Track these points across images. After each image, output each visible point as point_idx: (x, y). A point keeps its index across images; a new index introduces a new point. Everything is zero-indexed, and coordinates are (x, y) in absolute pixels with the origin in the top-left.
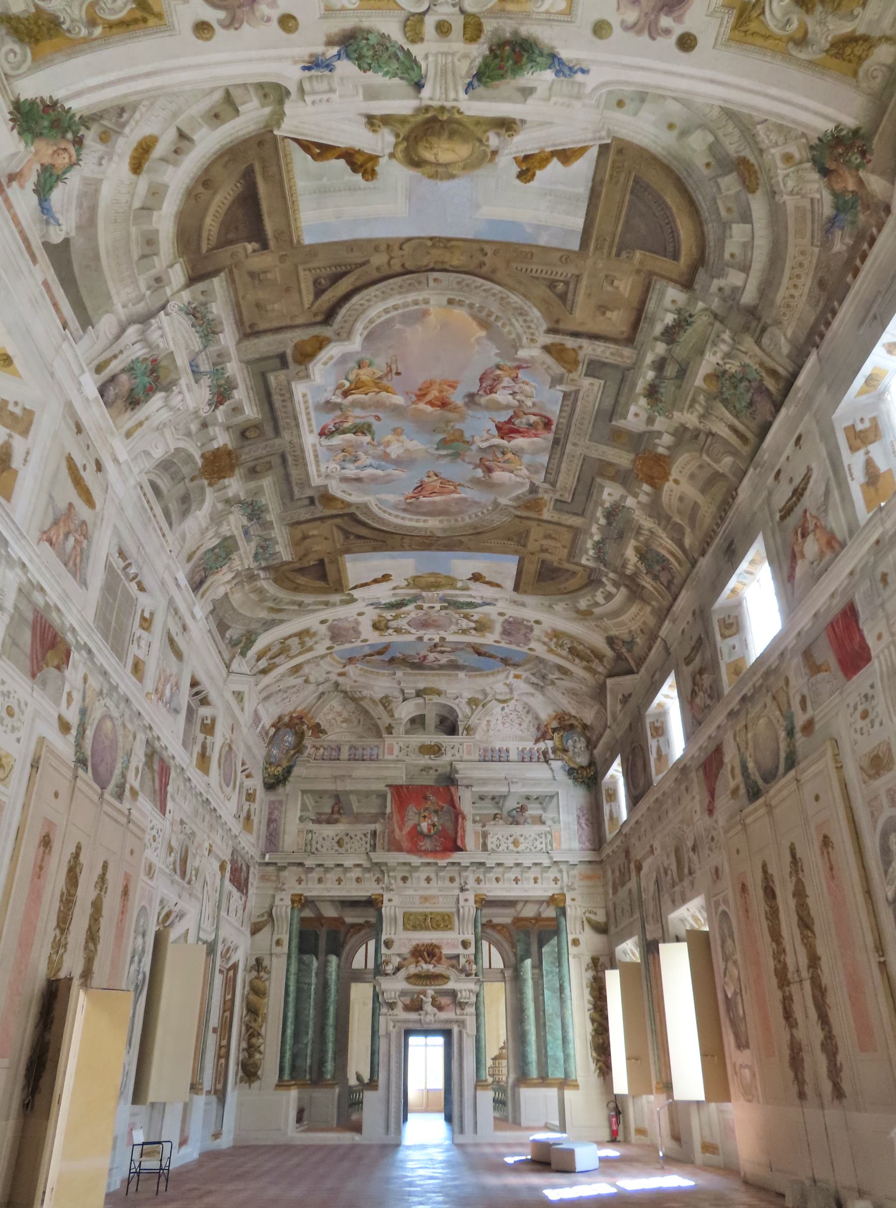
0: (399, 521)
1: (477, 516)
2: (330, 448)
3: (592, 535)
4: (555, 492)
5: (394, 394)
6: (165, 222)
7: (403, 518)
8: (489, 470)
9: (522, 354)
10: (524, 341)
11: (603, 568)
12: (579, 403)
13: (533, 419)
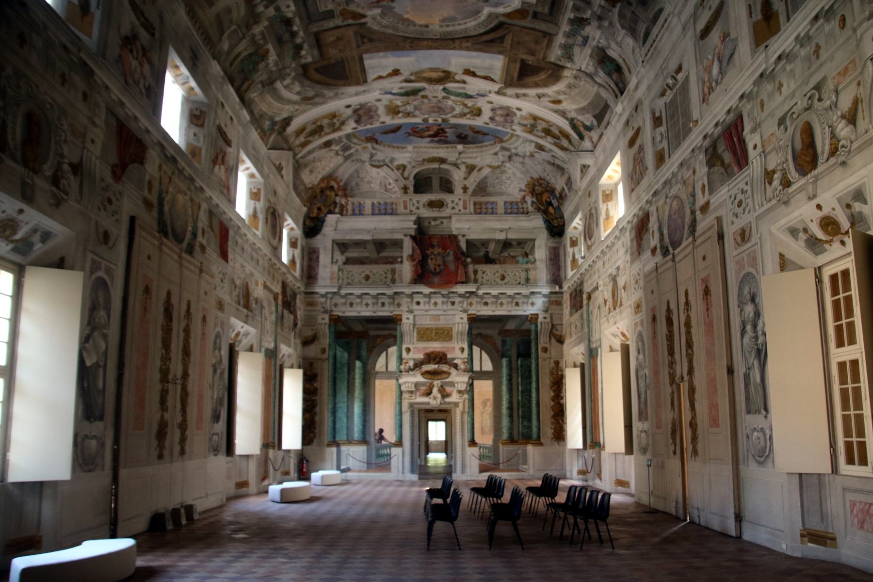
6: (560, 86)
9: (378, 11)
10: (379, 18)
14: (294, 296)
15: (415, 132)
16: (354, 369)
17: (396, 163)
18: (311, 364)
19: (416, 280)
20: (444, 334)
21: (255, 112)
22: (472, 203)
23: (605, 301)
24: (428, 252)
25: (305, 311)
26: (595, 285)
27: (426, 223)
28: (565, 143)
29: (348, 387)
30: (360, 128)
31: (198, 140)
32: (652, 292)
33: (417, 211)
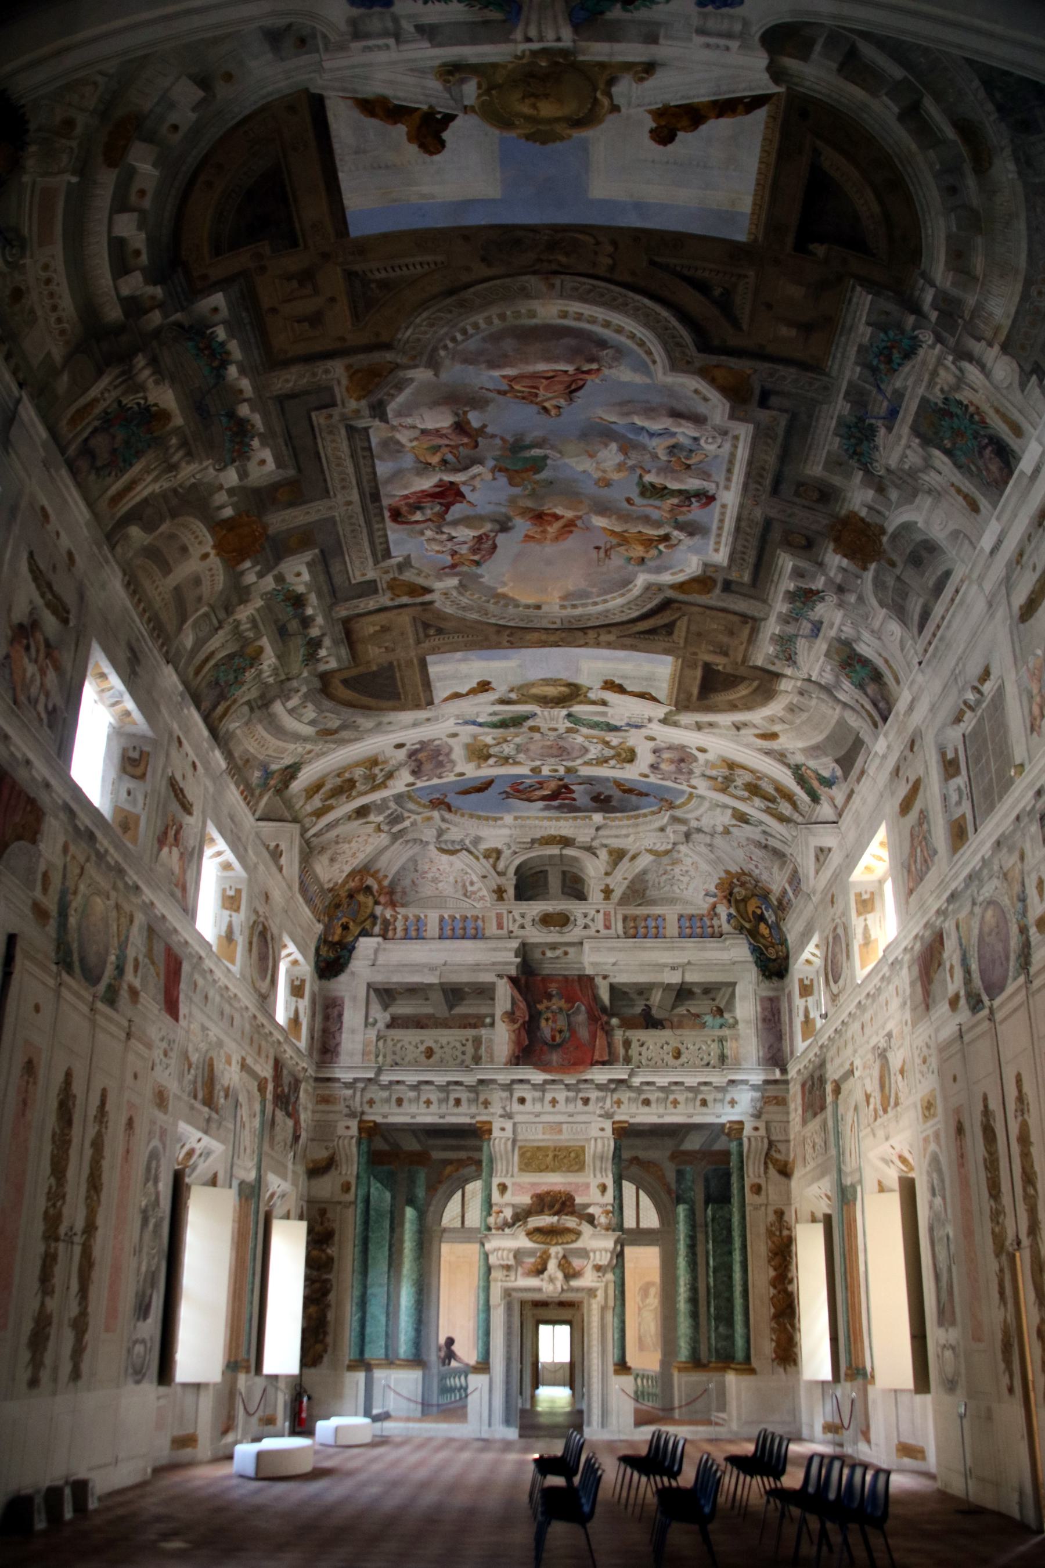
0: (617, 319)
1: (464, 332)
2: (706, 476)
3: (242, 371)
4: (344, 418)
5: (605, 529)
6: (775, 708)
7: (607, 324)
8: (461, 427)
10: (455, 593)
11: (178, 316)
12: (368, 551)
13: (418, 516)
14: (296, 1083)
15: (518, 791)
16: (402, 1224)
17: (483, 846)
18: (323, 1212)
19: (518, 1058)
20: (570, 1158)
21: (236, 755)
22: (620, 917)
23: (868, 1097)
24: (540, 1007)
25: (313, 1112)
26: (847, 1067)
27: (537, 955)
28: (785, 808)
29: (390, 1256)
30: (420, 784)
31: (134, 802)
32: (955, 1079)
33: (521, 932)
